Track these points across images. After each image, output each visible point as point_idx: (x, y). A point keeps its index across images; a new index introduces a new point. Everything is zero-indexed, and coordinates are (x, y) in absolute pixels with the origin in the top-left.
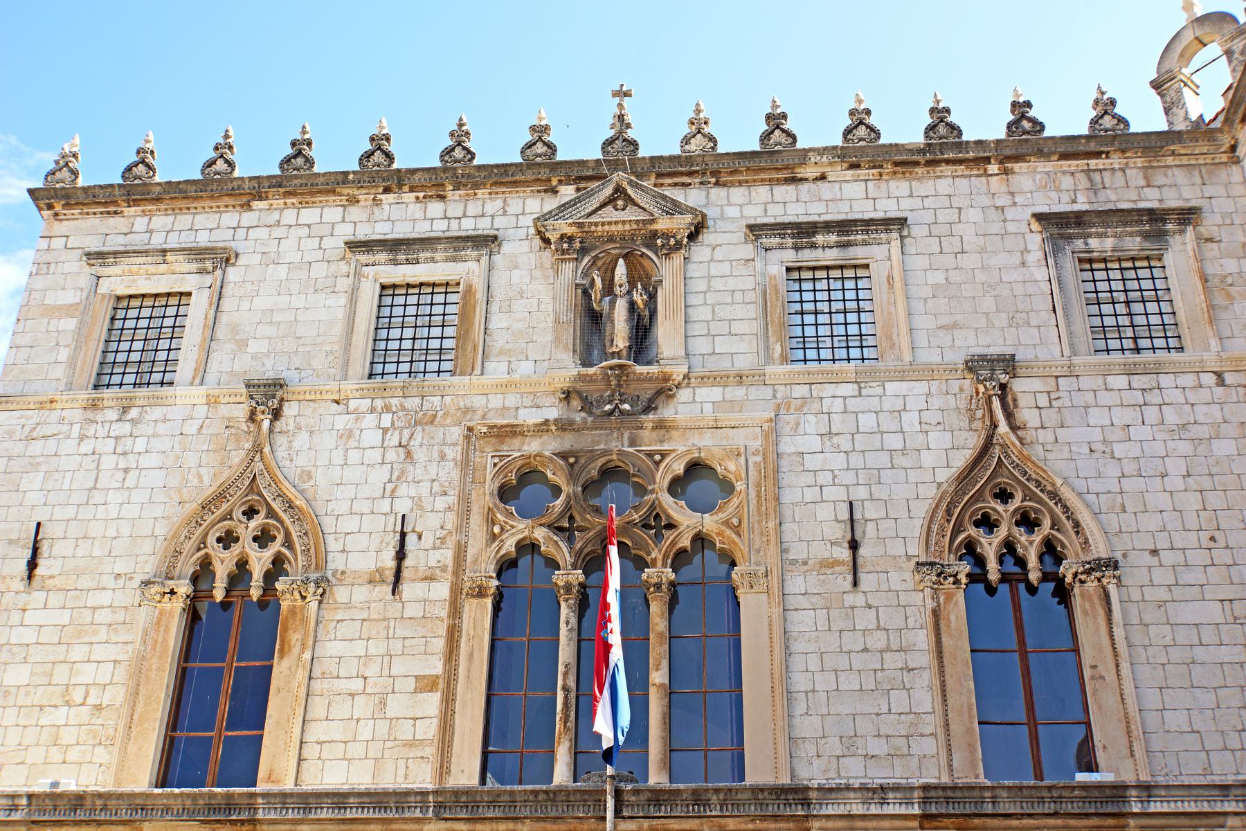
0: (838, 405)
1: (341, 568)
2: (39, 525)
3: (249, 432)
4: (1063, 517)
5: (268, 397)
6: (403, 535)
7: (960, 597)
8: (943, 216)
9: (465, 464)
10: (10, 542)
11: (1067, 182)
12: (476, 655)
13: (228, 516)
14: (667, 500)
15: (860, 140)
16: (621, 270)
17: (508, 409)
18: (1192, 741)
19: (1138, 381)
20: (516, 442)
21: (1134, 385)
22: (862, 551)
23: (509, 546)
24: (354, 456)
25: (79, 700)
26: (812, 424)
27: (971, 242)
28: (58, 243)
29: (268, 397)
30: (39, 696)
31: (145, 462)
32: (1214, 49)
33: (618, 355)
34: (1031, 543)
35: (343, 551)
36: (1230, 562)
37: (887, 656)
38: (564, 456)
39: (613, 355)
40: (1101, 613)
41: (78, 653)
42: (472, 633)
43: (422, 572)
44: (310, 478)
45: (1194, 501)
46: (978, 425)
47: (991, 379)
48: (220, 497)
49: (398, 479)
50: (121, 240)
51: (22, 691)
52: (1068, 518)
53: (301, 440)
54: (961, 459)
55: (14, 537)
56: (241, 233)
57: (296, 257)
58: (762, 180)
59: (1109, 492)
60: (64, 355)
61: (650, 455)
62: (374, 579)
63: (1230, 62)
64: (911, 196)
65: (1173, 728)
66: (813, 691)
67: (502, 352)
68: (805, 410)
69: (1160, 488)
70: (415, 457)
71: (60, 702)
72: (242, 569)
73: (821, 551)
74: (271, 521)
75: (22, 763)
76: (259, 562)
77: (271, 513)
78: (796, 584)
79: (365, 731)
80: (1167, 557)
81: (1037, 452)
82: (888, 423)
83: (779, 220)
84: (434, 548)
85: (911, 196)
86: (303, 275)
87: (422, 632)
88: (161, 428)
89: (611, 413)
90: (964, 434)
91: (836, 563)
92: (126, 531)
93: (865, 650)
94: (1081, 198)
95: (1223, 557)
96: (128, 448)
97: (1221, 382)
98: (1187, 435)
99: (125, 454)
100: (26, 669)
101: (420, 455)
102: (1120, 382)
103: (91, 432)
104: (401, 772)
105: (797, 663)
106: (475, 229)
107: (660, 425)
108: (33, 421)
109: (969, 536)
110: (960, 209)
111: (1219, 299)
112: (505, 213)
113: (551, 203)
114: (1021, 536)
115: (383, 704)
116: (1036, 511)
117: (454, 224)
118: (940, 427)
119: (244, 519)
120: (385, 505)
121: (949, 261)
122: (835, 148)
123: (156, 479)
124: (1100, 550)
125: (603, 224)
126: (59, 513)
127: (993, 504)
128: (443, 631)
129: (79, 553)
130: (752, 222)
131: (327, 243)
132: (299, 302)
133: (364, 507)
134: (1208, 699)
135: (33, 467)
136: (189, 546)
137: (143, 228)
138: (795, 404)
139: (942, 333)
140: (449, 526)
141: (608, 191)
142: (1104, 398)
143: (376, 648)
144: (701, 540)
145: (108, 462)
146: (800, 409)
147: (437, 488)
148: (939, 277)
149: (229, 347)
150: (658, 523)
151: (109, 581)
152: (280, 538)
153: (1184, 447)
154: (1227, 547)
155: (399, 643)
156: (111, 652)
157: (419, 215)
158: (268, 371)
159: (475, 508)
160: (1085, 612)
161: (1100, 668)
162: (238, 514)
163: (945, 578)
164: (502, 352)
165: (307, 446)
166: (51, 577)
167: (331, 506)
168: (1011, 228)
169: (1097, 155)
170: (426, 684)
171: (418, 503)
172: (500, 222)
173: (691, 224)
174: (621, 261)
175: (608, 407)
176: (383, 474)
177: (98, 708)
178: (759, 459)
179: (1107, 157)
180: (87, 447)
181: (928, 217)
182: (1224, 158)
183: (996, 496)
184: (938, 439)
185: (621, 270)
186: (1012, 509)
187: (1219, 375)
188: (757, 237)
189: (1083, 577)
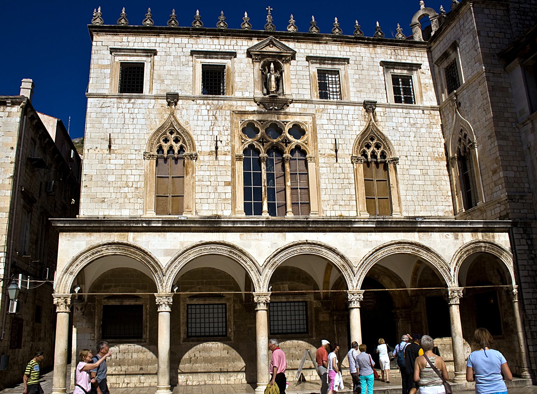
0: (332, 111)
1: (200, 150)
3: (168, 108)
5: (173, 99)
6: (217, 141)
9: (232, 122)
10: (102, 139)
11: (389, 52)
13: (165, 133)
14: (288, 135)
16: (272, 66)
20: (246, 116)
22: (338, 152)
23: (247, 146)
24: (200, 118)
25: (131, 186)
26: (325, 116)
27: (365, 67)
28: (99, 44)
29: (173, 99)
30: (119, 184)
31: (139, 116)
37: (344, 180)
38: (260, 121)
40: (394, 171)
41: (128, 172)
46: (367, 120)
48: (162, 127)
50: (120, 44)
51: (114, 183)
54: (362, 129)
55: (103, 138)
56: (157, 44)
60: (108, 81)
61: (283, 122)
67: (240, 89)
71: (125, 186)
72: (171, 148)
73: (328, 152)
76: (176, 147)
77: (178, 133)
78: (321, 160)
80: (409, 158)
81: (380, 128)
82: (345, 118)
86: (178, 60)
89: (272, 109)
90: (364, 122)
91: (332, 155)
93: (339, 178)
94: (393, 57)
95: (421, 158)
96: (133, 112)
97: (423, 113)
100: (114, 177)
101: (219, 118)
102: (400, 110)
103: (120, 106)
104: (223, 207)
105: (322, 181)
107: (286, 114)
112: (237, 45)
115: (216, 189)
117: (222, 47)
120: (211, 133)
126: (115, 130)
129: (123, 143)
131: (184, 50)
132: (178, 68)
133: (205, 133)
134: (416, 193)
135: (105, 116)
137: (126, 41)
138: (321, 110)
139: (358, 93)
140: (229, 140)
143: (213, 173)
144: (298, 147)
145: (127, 116)
147: (225, 128)
148: (357, 77)
149: (159, 81)
150: (287, 142)
153: (414, 130)
156: (138, 172)
157: (211, 43)
158: (173, 89)
159: (236, 135)
162: (168, 133)
164: (240, 89)
166: (116, 150)
167: (195, 132)
168: (375, 64)
169: (397, 45)
170: (227, 184)
171: (220, 132)
172: (236, 48)
177: (137, 188)
178: (312, 125)
180: (120, 111)
183: (370, 139)
184: (357, 123)
185: (272, 66)
187: (423, 111)
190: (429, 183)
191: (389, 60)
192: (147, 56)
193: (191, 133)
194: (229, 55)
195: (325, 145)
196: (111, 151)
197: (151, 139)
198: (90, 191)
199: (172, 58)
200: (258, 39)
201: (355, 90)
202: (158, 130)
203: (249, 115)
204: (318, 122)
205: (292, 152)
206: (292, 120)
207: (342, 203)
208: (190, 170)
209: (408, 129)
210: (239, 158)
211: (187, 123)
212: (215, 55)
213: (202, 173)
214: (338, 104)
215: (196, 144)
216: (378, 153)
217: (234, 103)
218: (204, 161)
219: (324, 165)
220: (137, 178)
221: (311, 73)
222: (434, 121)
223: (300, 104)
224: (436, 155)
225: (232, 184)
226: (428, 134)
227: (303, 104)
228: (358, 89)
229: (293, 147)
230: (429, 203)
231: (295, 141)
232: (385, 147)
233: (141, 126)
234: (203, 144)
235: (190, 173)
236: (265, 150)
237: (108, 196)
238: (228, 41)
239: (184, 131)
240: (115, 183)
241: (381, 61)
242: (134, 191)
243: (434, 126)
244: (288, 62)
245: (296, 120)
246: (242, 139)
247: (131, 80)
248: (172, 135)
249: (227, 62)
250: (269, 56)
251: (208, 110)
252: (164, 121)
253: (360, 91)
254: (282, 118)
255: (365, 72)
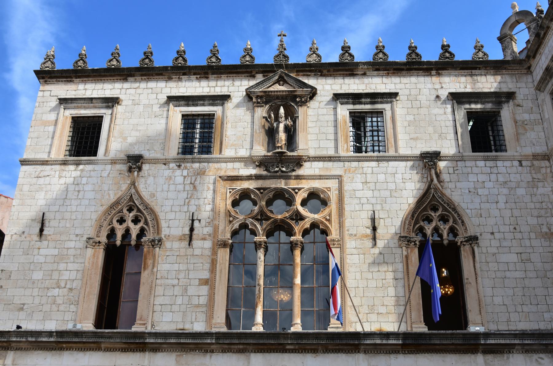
0: (370, 170)
1: (168, 233)
2: (44, 213)
3: (129, 176)
4: (457, 218)
6: (193, 221)
7: (416, 251)
8: (413, 92)
12: (223, 271)
15: (380, 58)
16: (282, 111)
17: (235, 169)
18: (503, 309)
19: (489, 163)
20: (239, 183)
21: (487, 165)
22: (379, 231)
23: (236, 226)
24: (172, 187)
25: (63, 285)
26: (359, 178)
28: (47, 94)
30: (47, 283)
31: (87, 188)
32: (522, 26)
33: (281, 147)
34: (445, 229)
35: (168, 227)
36: (521, 238)
38: (259, 189)
39: (278, 147)
41: (62, 266)
42: (221, 262)
43: (201, 236)
44: (154, 196)
45: (508, 213)
46: (425, 180)
47: (431, 161)
48: (117, 203)
49: (191, 197)
50: (74, 93)
51: (40, 282)
52: (459, 219)
53: (151, 180)
57: (147, 102)
58: (340, 74)
59: (476, 209)
61: (294, 189)
62: (181, 239)
63: (529, 32)
64: (400, 83)
65: (497, 303)
66: (358, 287)
68: (356, 172)
69: (495, 207)
70: (197, 188)
71: (55, 286)
72: (127, 233)
74: (139, 214)
75: (41, 311)
76: (135, 230)
77: (139, 210)
78: (350, 244)
79: (179, 301)
80: (497, 235)
81: (447, 192)
82: (390, 179)
83: (347, 92)
84: (206, 227)
85: (400, 83)
86: (150, 109)
87: (201, 261)
88: (92, 173)
89: (277, 172)
91: (367, 236)
92: (79, 217)
94: (468, 86)
95: (518, 236)
96: (79, 182)
97: (521, 165)
98: (507, 186)
99: (78, 184)
102: (481, 163)
103: (64, 175)
104: (194, 317)
106: (221, 92)
107: (298, 177)
108: (39, 170)
109: (421, 225)
110: (420, 89)
111: (521, 131)
113: (252, 83)
114: (441, 225)
115: (186, 290)
116: (448, 216)
117: (212, 89)
118: (411, 180)
119: (127, 213)
120: (185, 208)
121: (415, 111)
122: (370, 62)
123: (91, 195)
124: (471, 232)
125: (274, 91)
127: (430, 213)
128: (209, 261)
129: (61, 225)
130: (336, 92)
133: (177, 209)
134: (510, 292)
136: (105, 223)
141: (277, 78)
142: (475, 170)
143: (183, 267)
144: (314, 225)
146: (354, 172)
148: (411, 118)
151: (73, 237)
152: (143, 221)
153: (505, 191)
154: (520, 232)
155: (192, 266)
156: (76, 266)
160: (465, 257)
161: (470, 279)
162: (125, 211)
163: (411, 243)
164: (232, 145)
165: (153, 183)
166: (50, 235)
167: (163, 208)
169: (475, 69)
172: (232, 89)
173: (311, 92)
174: (282, 108)
175: (277, 169)
176: (185, 195)
177: (71, 289)
179: (479, 69)
181: (407, 92)
182: (525, 71)
183: (431, 209)
185: (282, 111)
186: (437, 215)
187: (520, 162)
188: (338, 99)
189: (465, 243)
190: (532, 275)
191: (462, 90)
192: (108, 107)
193: (157, 209)
194: (220, 100)
195: (356, 221)
196: (43, 237)
197: (100, 219)
198: (5, 294)
199: (141, 107)
200: (264, 76)
201: (407, 137)
202: (112, 207)
203: (243, 182)
204: (347, 187)
205: (305, 233)
206: (307, 185)
207: (383, 310)
208: (150, 262)
209: (495, 191)
210: (224, 245)
211: (153, 195)
212: (200, 100)
213: (166, 267)
214: (379, 160)
215: (163, 224)
216: (445, 229)
217: (223, 165)
218: (171, 250)
219: (355, 251)
220: (73, 275)
221: (339, 117)
222: (539, 176)
223: (320, 164)
224: (545, 229)
225: (208, 282)
226: (529, 197)
227: (326, 163)
228: (413, 136)
229: (308, 226)
230: (534, 308)
231: (310, 216)
232: (455, 221)
233: (87, 202)
234: (172, 225)
235: (150, 267)
236: (264, 230)
237: (29, 301)
238: (220, 83)
239: (147, 207)
240: (42, 283)
241: (450, 93)
242: (66, 293)
243: (540, 184)
244: (303, 103)
245: (314, 186)
246: (230, 216)
247: (85, 138)
248: (130, 212)
249: (217, 110)
250: (278, 97)
251: (185, 177)
252: (120, 193)
253: (416, 139)
254: (293, 184)
255: (423, 111)
